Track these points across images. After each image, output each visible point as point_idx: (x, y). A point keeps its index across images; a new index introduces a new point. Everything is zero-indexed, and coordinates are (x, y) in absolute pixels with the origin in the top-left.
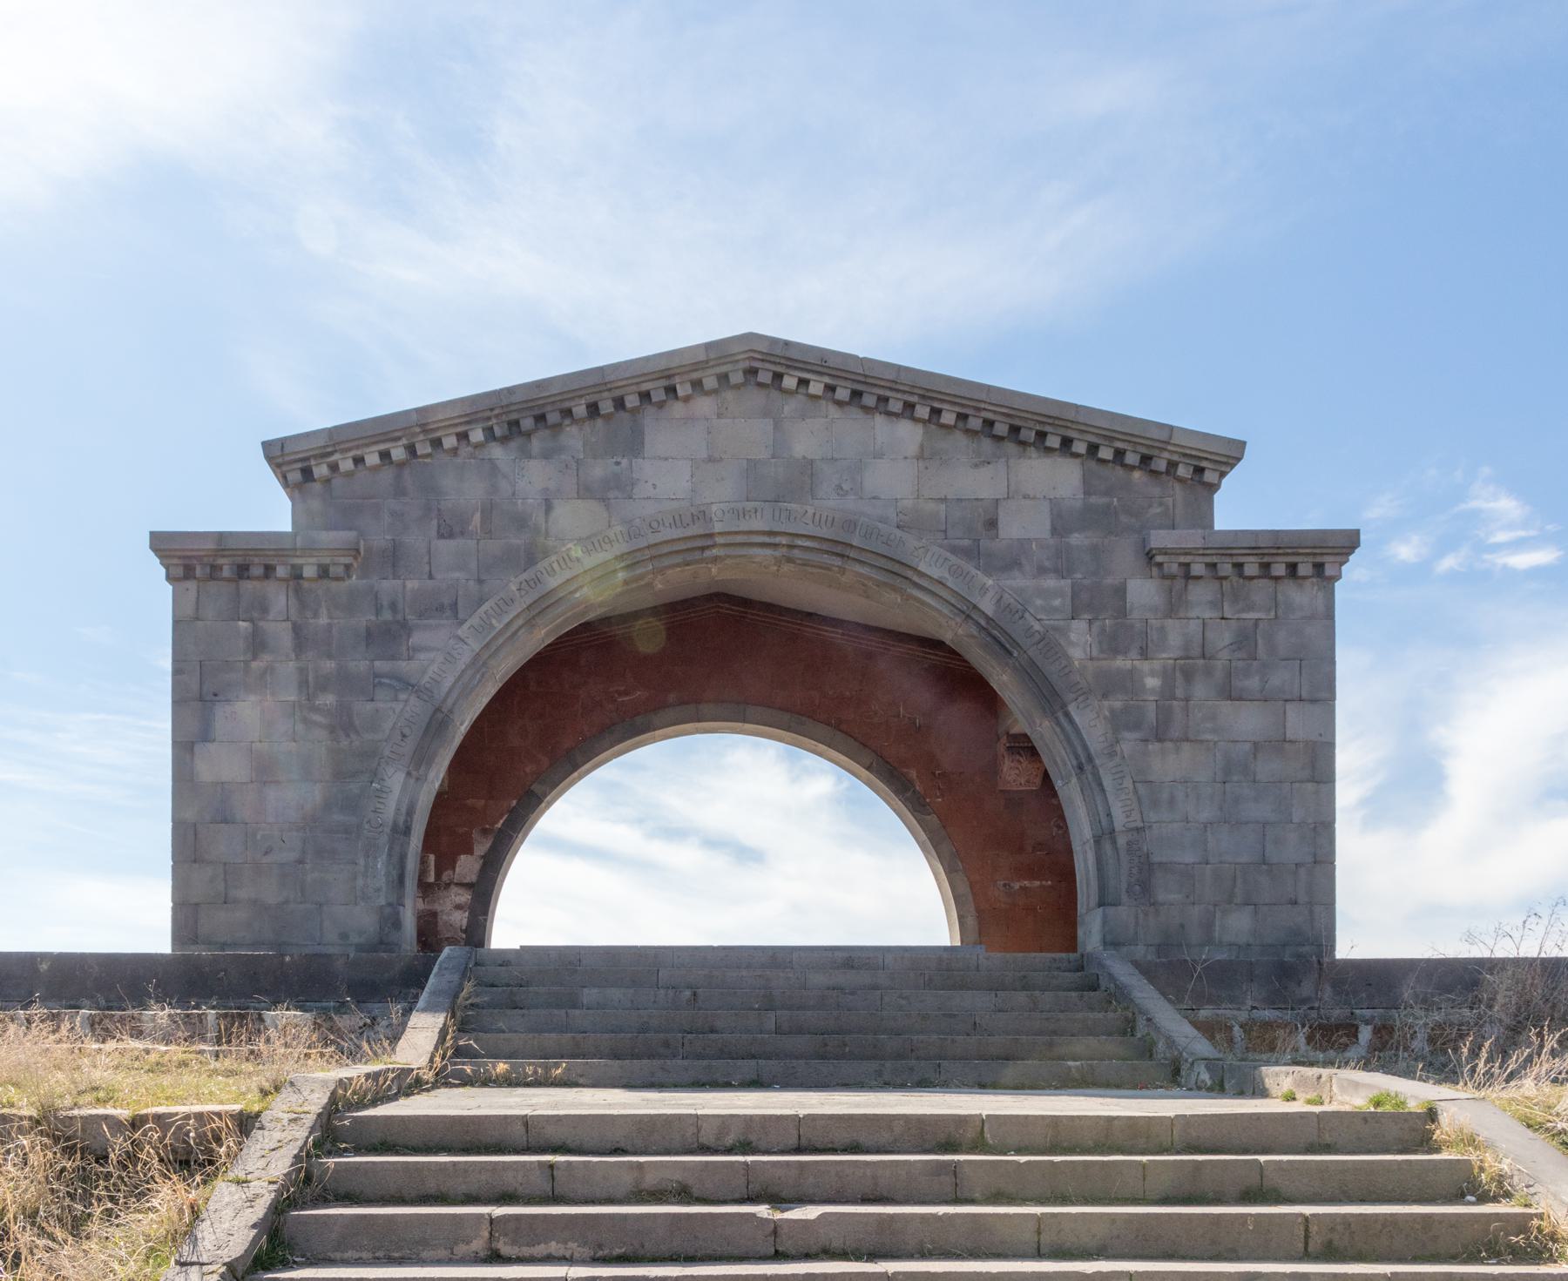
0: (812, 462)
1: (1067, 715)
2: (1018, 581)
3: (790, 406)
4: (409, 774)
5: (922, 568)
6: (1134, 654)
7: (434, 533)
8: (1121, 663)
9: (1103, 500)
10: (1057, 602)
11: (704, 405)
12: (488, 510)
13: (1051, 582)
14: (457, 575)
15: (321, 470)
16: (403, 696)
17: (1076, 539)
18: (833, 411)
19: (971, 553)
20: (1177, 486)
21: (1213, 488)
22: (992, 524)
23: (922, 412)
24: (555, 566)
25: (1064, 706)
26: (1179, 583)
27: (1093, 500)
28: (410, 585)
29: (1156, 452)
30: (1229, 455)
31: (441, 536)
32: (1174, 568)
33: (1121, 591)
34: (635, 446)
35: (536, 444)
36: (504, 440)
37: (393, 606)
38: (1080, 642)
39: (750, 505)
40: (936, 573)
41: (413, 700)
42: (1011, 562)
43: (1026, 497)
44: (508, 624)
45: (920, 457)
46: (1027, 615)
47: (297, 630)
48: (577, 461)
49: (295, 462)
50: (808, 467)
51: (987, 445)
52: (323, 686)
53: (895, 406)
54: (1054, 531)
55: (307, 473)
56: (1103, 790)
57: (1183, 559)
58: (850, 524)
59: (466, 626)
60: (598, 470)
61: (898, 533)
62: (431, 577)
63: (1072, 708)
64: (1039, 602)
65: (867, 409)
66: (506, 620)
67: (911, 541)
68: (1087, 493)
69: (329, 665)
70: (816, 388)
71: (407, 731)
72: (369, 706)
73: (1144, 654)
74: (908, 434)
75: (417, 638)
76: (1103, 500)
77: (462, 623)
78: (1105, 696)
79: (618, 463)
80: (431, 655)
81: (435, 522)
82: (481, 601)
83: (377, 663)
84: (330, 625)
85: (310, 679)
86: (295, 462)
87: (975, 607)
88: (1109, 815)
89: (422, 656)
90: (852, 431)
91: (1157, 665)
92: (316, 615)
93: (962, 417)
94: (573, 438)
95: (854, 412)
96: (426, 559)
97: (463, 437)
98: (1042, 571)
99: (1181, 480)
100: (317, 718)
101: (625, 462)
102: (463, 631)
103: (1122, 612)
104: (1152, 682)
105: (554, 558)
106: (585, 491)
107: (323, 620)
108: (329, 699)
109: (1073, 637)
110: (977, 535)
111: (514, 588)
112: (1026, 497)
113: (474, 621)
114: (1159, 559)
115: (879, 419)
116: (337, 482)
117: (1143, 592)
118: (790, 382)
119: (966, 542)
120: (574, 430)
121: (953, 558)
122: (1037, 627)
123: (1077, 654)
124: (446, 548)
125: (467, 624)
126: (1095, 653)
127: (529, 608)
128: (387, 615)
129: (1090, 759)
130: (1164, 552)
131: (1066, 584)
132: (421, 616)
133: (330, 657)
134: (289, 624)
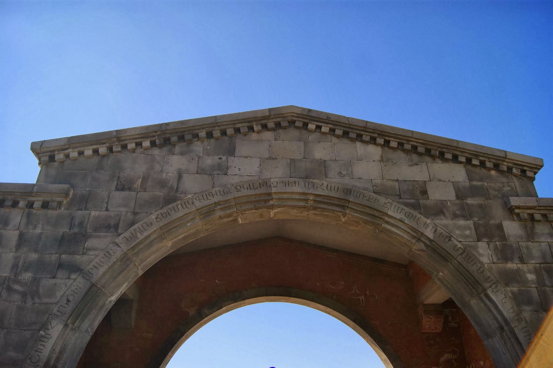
2: (443, 222)
3: (312, 137)
4: (66, 326)
5: (390, 213)
6: (516, 260)
7: (113, 188)
8: (510, 266)
9: (479, 183)
10: (468, 232)
11: (268, 135)
12: (145, 179)
13: (462, 222)
14: (122, 209)
15: (60, 156)
16: (73, 276)
17: (470, 201)
18: (335, 140)
19: (416, 206)
20: (514, 178)
21: (533, 179)
22: (424, 192)
23: (381, 141)
24: (180, 206)
25: (485, 290)
26: (529, 224)
27: (475, 183)
28: (93, 213)
29: (500, 162)
31: (117, 189)
33: (500, 227)
34: (231, 152)
35: (177, 149)
36: (161, 147)
37: (81, 224)
38: (485, 253)
40: (398, 216)
41: (80, 280)
42: (438, 210)
43: (439, 180)
45: (382, 160)
46: (452, 239)
47: (21, 236)
48: (199, 157)
49: (45, 152)
50: (323, 163)
51: (415, 157)
52: (26, 269)
53: (366, 138)
54: (458, 197)
55: (52, 158)
58: (348, 191)
60: (209, 161)
61: (374, 195)
62: (107, 210)
63: (489, 292)
64: (458, 232)
65: (352, 140)
66: (146, 234)
67: (382, 200)
68: (470, 180)
69: (34, 256)
70: (325, 129)
71: (71, 298)
72: (52, 281)
73: (522, 261)
74: (375, 151)
75: (90, 243)
76: (479, 183)
77: (119, 235)
78: (507, 285)
79: (220, 158)
80: (97, 253)
81: (115, 183)
82: (133, 224)
83: (63, 256)
84: (41, 233)
85: (20, 264)
86: (45, 152)
87: (422, 234)
89: (91, 253)
90: (345, 149)
91: (531, 267)
92: (35, 228)
93: (401, 144)
94: (198, 147)
95: (345, 141)
96: (106, 201)
97: (139, 144)
98: (455, 216)
99: (516, 176)
100: (17, 287)
101: (224, 158)
102: (119, 240)
103: (503, 237)
104: (531, 277)
105: (179, 202)
106: (200, 171)
107: (38, 231)
108: (27, 276)
109: (481, 251)
110: (415, 197)
111: (153, 217)
112: (439, 180)
113: (127, 234)
114: (517, 211)
115: (358, 144)
116: (68, 162)
117: (512, 228)
118: (312, 126)
119: (412, 201)
120: (199, 143)
121: (405, 208)
122: (459, 245)
123: (485, 260)
124: (118, 196)
125: (122, 236)
126: (495, 260)
128: (76, 230)
130: (518, 207)
131: (470, 223)
132: (96, 230)
133: (36, 251)
134: (17, 232)
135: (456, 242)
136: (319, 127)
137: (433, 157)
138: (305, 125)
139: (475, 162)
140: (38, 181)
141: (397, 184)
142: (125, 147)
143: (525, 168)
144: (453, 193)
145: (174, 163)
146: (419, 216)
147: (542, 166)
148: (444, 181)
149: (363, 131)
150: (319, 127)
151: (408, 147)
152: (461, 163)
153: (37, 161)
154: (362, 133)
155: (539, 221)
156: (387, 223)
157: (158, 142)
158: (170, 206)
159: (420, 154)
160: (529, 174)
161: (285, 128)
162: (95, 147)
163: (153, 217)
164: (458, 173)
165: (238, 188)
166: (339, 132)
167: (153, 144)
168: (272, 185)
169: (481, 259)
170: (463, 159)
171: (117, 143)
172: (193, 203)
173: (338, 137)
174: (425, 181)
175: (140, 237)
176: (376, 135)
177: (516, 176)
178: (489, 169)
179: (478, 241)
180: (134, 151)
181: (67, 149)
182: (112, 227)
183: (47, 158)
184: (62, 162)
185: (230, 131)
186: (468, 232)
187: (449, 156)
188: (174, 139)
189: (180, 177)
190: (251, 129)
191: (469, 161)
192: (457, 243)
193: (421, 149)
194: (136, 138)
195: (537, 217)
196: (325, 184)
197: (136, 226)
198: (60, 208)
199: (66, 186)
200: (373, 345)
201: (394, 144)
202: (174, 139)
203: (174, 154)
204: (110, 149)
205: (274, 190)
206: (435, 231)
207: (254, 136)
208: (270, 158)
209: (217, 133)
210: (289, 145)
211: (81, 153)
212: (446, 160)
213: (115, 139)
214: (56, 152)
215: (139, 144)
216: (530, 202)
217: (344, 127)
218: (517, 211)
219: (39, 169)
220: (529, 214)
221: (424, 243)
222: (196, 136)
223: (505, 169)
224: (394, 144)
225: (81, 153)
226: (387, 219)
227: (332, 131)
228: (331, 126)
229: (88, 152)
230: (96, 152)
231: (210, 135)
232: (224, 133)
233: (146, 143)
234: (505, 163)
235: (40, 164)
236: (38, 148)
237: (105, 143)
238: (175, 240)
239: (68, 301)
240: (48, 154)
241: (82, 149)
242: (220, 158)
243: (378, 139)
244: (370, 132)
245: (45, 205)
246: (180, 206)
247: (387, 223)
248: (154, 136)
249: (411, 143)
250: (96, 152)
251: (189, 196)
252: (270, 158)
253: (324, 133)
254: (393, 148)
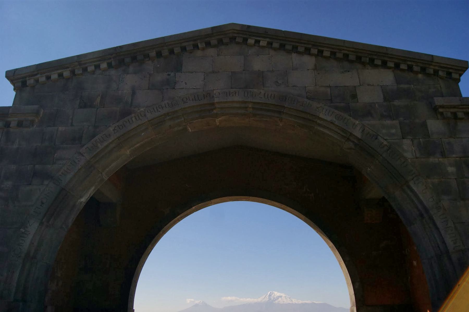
0: (263, 72)
1: (409, 187)
4: (41, 223)
5: (321, 116)
8: (432, 160)
9: (406, 86)
10: (393, 131)
11: (211, 52)
13: (388, 122)
15: (31, 82)
16: (46, 182)
17: (396, 103)
18: (272, 52)
21: (459, 80)
22: (354, 96)
23: (314, 51)
24: (134, 119)
28: (60, 128)
30: (460, 67)
31: (80, 107)
32: (449, 114)
33: (424, 125)
34: (178, 68)
35: (131, 69)
38: (409, 149)
39: (232, 90)
40: (329, 118)
42: (367, 112)
43: (369, 85)
44: (107, 146)
45: (315, 68)
46: (379, 137)
53: (301, 49)
54: (385, 99)
55: (24, 84)
56: (437, 228)
57: (452, 110)
59: (84, 148)
60: (159, 78)
62: (72, 125)
63: (411, 184)
64: (384, 131)
65: (289, 52)
66: (105, 144)
70: (263, 43)
73: (443, 155)
74: (309, 61)
76: (406, 86)
79: (169, 75)
82: (94, 136)
83: (37, 166)
88: (444, 242)
90: (281, 60)
93: (333, 53)
94: (149, 66)
97: (97, 67)
99: (441, 78)
101: (172, 74)
104: (451, 169)
105: (133, 115)
107: (15, 146)
108: (8, 184)
110: (345, 101)
111: (111, 129)
112: (369, 85)
114: (441, 110)
115: (294, 55)
117: (435, 126)
118: (251, 41)
119: (342, 104)
120: (150, 62)
121: (336, 111)
122: (385, 143)
123: (408, 155)
125: (85, 146)
126: (418, 155)
127: (118, 138)
129: (427, 211)
130: (442, 107)
131: (396, 122)
135: (382, 140)
136: (257, 42)
137: (364, 64)
138: (245, 40)
139: (403, 66)
140: (13, 104)
141: (329, 90)
142: (85, 70)
143: (451, 71)
144: (382, 96)
145: (129, 81)
146: (349, 117)
147: (467, 68)
148: (373, 85)
149: (298, 42)
150: (257, 42)
151: (339, 55)
152: (389, 68)
153: (13, 87)
154: (298, 44)
155: (462, 119)
156: (320, 125)
157: (113, 63)
158: (126, 119)
159: (352, 62)
160: (455, 76)
161: (227, 44)
162: (59, 71)
163: (111, 129)
164: (387, 78)
165: (185, 100)
166: (276, 45)
167: (110, 65)
168: (214, 96)
169: (406, 154)
170: (391, 65)
171: (78, 67)
172: (145, 115)
173: (275, 49)
174: (355, 87)
175: (101, 147)
176: (310, 46)
177: (441, 78)
178: (417, 73)
179: (403, 138)
180: (93, 72)
181: (36, 75)
182: (76, 139)
183: (20, 84)
184: (33, 87)
185: (177, 50)
186: (393, 131)
187: (378, 62)
188: (128, 60)
189: (134, 93)
190: (196, 47)
191: (397, 66)
192: (382, 140)
193: (352, 57)
194: (94, 62)
195: (460, 115)
196: (263, 92)
197: (96, 138)
198: (33, 126)
199: (36, 107)
200: (322, 235)
201: (327, 53)
202: (128, 60)
203: (128, 73)
204: (73, 72)
205: (216, 100)
206: (363, 131)
207: (199, 53)
208: (213, 72)
209: (165, 52)
210: (230, 59)
211: (48, 78)
212: (376, 66)
213: (77, 63)
214: (27, 78)
215: (97, 67)
216: (455, 101)
217: (280, 40)
218: (441, 110)
219: (14, 93)
220: (452, 113)
221: (353, 142)
222: (147, 56)
223: (431, 71)
224: (326, 54)
225: (48, 78)
226: (319, 121)
227: (270, 44)
228: (268, 40)
229: (54, 76)
230: (61, 75)
231: (159, 55)
232: (172, 52)
233: (104, 65)
234: (432, 67)
235: (14, 89)
236: (12, 76)
237: (68, 68)
238: (132, 148)
239: (42, 203)
240: (21, 80)
241: (48, 74)
242: (169, 75)
243: (312, 49)
244: (305, 44)
245: (20, 124)
246: (134, 119)
247: (320, 125)
248: (110, 59)
249: (343, 51)
250: (61, 75)
251: (142, 109)
252: (213, 72)
253: (263, 47)
254: (325, 57)
